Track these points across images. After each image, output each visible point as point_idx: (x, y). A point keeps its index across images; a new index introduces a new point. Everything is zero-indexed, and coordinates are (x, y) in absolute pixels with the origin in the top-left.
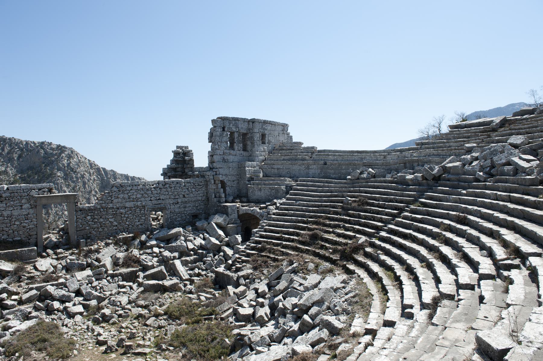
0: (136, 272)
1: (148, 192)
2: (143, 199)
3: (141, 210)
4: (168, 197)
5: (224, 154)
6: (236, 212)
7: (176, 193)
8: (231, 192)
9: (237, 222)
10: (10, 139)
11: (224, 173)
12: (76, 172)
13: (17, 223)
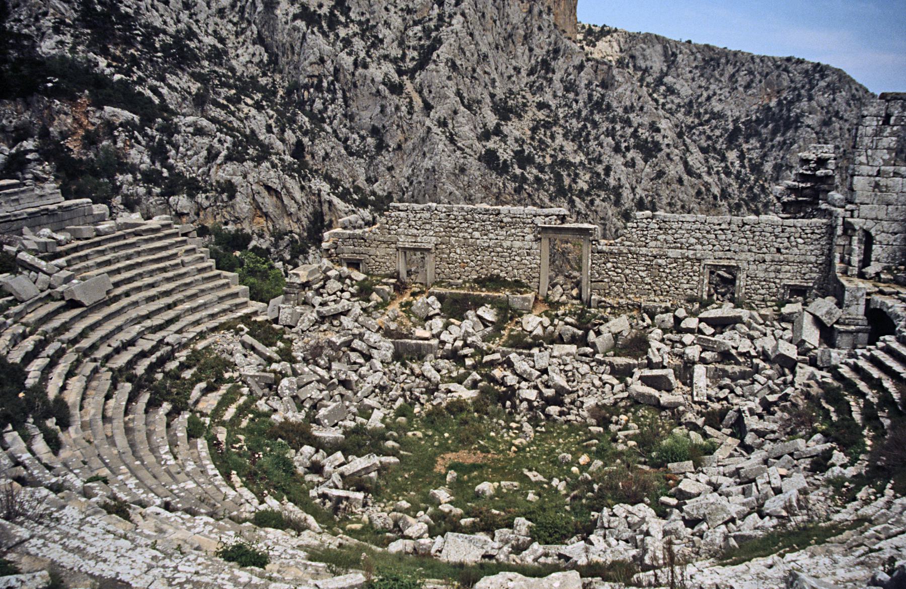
0: (634, 366)
1: (708, 236)
2: (699, 247)
3: (692, 266)
4: (746, 248)
5: (879, 173)
6: (862, 302)
7: (762, 243)
8: (885, 255)
9: (860, 322)
10: (735, 54)
11: (873, 215)
12: (841, 118)
13: (517, 258)
